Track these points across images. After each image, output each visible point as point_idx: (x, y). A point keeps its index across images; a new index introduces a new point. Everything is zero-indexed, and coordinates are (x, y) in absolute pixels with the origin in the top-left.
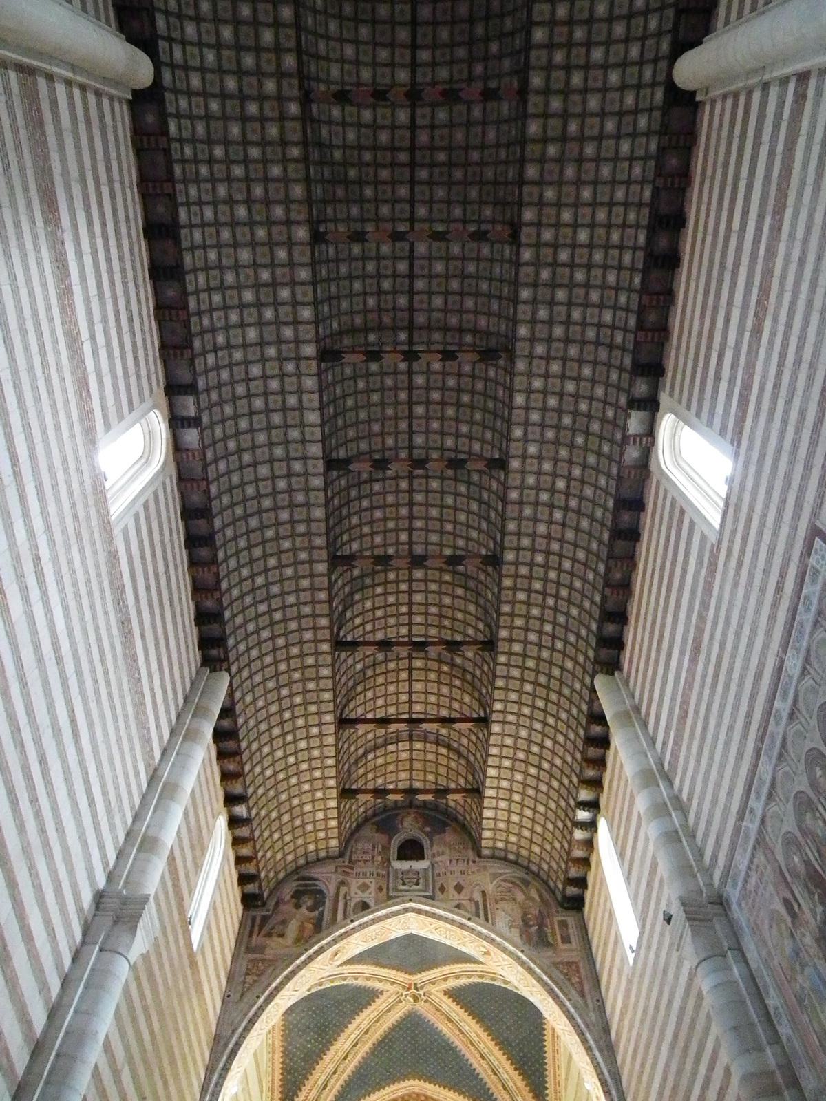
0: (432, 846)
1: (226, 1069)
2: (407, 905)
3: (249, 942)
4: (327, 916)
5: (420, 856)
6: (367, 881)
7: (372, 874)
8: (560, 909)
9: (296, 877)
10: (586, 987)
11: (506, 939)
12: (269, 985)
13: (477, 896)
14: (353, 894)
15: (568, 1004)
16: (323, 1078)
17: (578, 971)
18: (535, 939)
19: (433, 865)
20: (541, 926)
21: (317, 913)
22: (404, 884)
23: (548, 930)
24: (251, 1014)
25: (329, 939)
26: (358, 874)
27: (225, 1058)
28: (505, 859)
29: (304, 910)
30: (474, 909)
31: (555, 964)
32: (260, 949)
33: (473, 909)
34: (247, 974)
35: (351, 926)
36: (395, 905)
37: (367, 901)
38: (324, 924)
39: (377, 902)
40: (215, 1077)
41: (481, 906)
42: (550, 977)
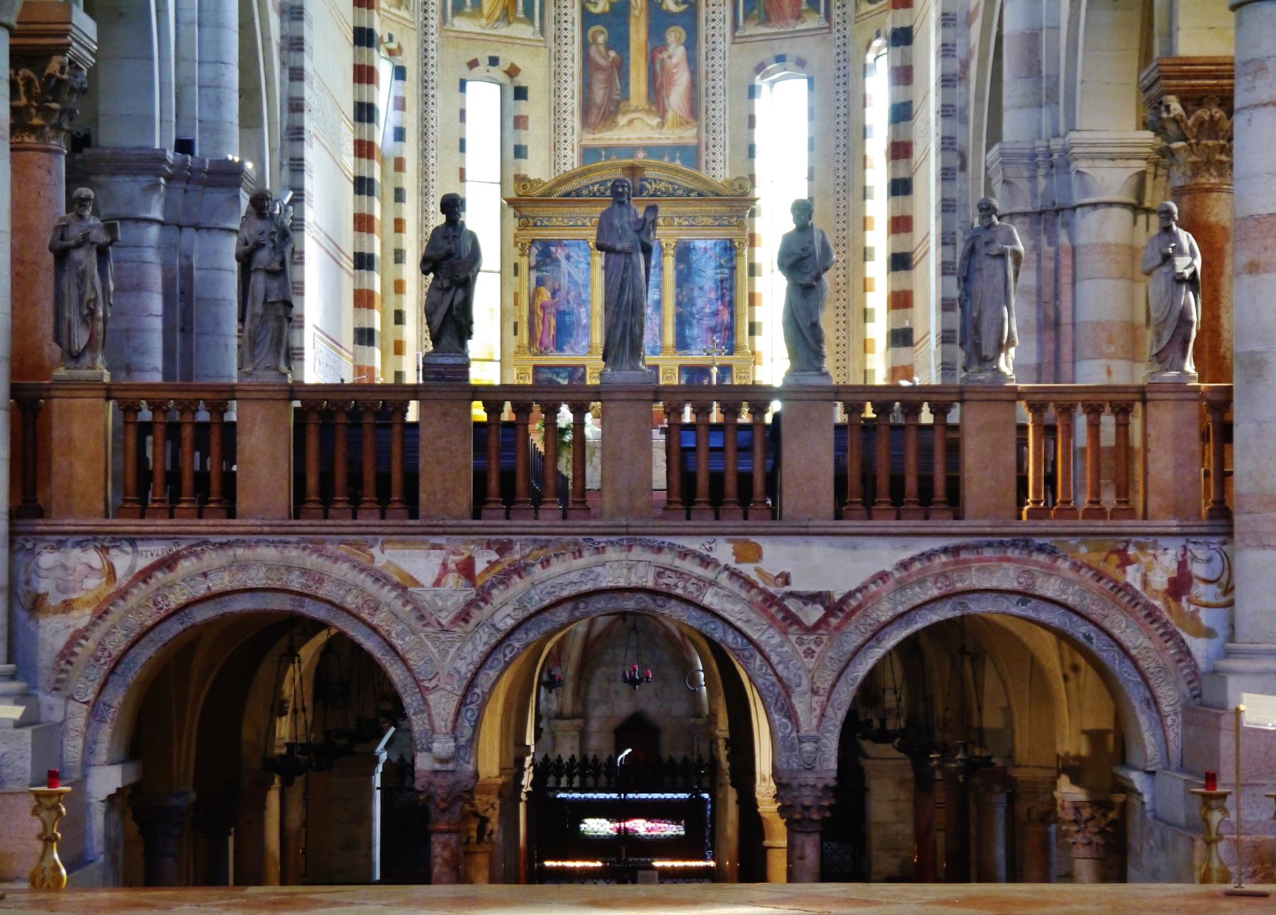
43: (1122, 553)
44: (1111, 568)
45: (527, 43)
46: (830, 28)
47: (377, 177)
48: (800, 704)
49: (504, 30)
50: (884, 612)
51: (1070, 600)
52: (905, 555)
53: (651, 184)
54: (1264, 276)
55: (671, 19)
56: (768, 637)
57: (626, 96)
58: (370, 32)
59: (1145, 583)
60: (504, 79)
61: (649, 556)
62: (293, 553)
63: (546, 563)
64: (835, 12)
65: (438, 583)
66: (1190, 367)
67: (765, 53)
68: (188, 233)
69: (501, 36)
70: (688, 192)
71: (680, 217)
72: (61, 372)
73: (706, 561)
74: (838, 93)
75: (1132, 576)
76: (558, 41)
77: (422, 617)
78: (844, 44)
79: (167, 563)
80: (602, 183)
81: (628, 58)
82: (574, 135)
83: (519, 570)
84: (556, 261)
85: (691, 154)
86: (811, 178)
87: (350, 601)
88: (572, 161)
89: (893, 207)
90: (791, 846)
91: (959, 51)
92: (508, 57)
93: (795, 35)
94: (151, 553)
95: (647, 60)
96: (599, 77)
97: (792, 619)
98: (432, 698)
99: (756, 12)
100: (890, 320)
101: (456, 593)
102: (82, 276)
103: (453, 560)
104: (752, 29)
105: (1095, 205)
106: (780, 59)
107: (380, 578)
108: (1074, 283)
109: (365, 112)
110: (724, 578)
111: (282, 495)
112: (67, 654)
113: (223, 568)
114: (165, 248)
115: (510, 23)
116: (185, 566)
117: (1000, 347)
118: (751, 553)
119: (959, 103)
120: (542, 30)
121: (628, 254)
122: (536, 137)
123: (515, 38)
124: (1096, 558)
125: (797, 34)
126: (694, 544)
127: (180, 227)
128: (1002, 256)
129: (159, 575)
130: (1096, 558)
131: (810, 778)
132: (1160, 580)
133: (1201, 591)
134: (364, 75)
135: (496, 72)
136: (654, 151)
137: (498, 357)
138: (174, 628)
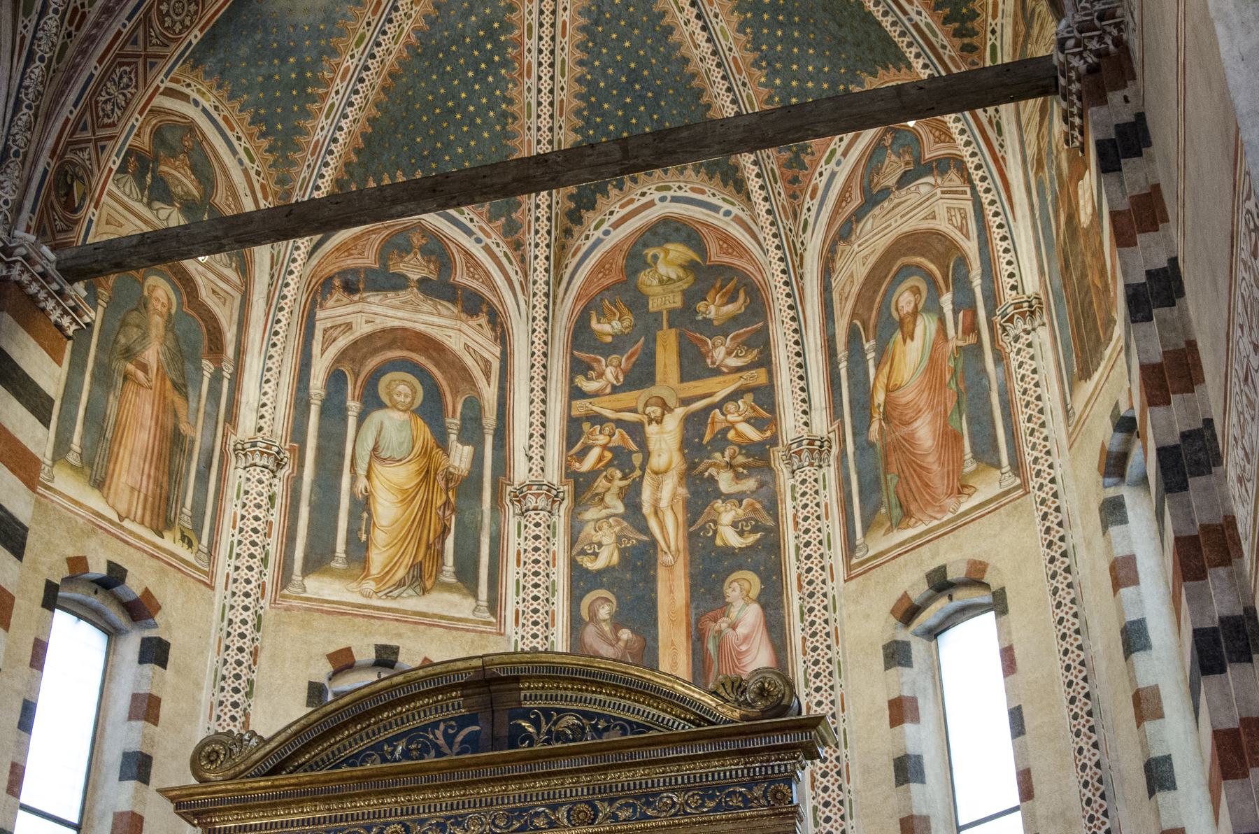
45: (460, 625)
46: (1024, 485)
49: (411, 602)
53: (536, 723)
55: (732, 560)
69: (405, 612)
71: (611, 801)
74: (1055, 591)
76: (521, 620)
78: (1055, 495)
81: (656, 639)
93: (959, 523)
95: (689, 636)
99: (883, 510)
104: (880, 542)
115: (425, 591)
120: (494, 605)
123: (434, 616)
125: (960, 522)
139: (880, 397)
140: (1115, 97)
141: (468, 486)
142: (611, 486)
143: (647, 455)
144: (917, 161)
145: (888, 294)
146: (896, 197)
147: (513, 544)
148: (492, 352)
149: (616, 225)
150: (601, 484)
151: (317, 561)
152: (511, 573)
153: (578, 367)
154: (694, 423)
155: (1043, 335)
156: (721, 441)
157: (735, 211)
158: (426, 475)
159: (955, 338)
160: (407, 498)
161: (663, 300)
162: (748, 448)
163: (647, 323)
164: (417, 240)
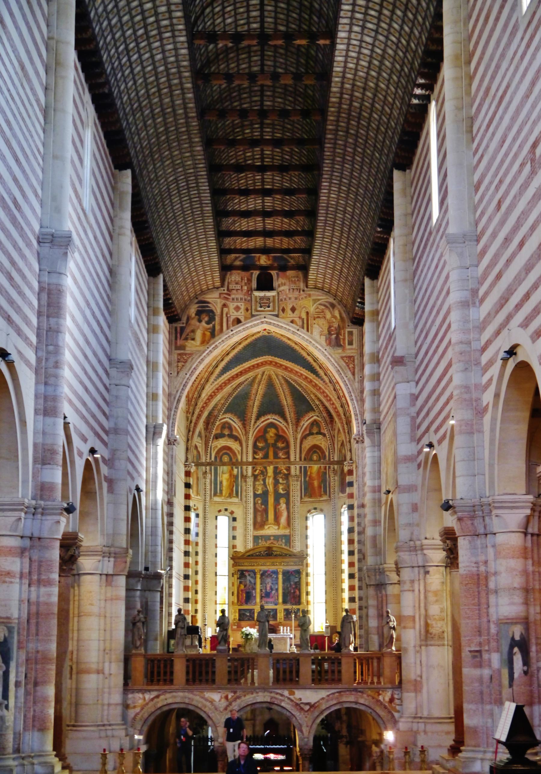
0: (278, 279)
1: (177, 408)
2: (263, 320)
3: (176, 343)
4: (217, 328)
5: (270, 288)
6: (239, 304)
7: (241, 299)
8: (350, 324)
9: (196, 301)
10: (356, 370)
11: (317, 342)
12: (191, 367)
13: (304, 316)
14: (231, 314)
15: (345, 379)
16: (215, 362)
17: (354, 361)
18: (333, 342)
19: (278, 293)
20: (338, 334)
21: (211, 325)
22: (261, 307)
23: (341, 337)
24: (184, 382)
25: (220, 341)
26: (233, 299)
27: (175, 403)
28: (322, 290)
29: (203, 323)
30: (301, 323)
31: (342, 358)
32: (183, 347)
33: (299, 322)
34: (178, 362)
35: (232, 333)
36: (256, 320)
37: (240, 317)
38: (216, 333)
39: (246, 318)
40: (173, 413)
41: (305, 322)
42: (338, 364)
43: (378, 692)
44: (376, 696)
47: (191, 550)
48: (305, 729)
49: (229, 500)
50: (324, 707)
51: (367, 703)
52: (328, 693)
54: (407, 630)
55: (282, 496)
56: (297, 713)
57: (267, 520)
58: (189, 506)
59: (384, 699)
60: (230, 515)
61: (269, 694)
62: (186, 694)
63: (245, 696)
64: (332, 495)
65: (220, 701)
66: (394, 648)
67: (310, 507)
68: (147, 592)
70: (286, 555)
72: (134, 652)
73: (282, 695)
75: (381, 698)
77: (216, 709)
79: (157, 697)
80: (260, 552)
82: (251, 532)
83: (239, 697)
84: (245, 576)
85: (288, 539)
86: (325, 546)
87: (200, 705)
88: (250, 545)
89: (349, 559)
90: (303, 764)
91: (363, 525)
92: (230, 508)
93: (320, 501)
94: (154, 694)
96: (259, 514)
97: (302, 709)
98: (218, 728)
100: (349, 594)
101: (224, 703)
102: (139, 629)
103: (224, 695)
104: (306, 499)
105: (391, 584)
106: (315, 509)
107: (206, 700)
108: (387, 604)
109: (187, 531)
110: (286, 699)
111: (184, 681)
112: (134, 719)
113: (170, 698)
114: (141, 596)
116: (162, 697)
117: (350, 644)
118: (293, 693)
119: (362, 540)
120: (241, 500)
121: (264, 622)
122: (239, 534)
124: (372, 694)
126: (279, 691)
127: (145, 591)
128: (350, 622)
129: (156, 700)
130: (372, 694)
131: (306, 747)
132: (387, 699)
133: (397, 702)
134: (187, 520)
135: (226, 513)
136: (277, 538)
137: (227, 602)
138: (159, 712)
139: (309, 473)
140: (351, 477)
141: (236, 477)
142: (261, 478)
143: (267, 473)
144: (320, 430)
145: (312, 454)
146: (316, 436)
147: (244, 488)
148: (239, 449)
149: (262, 422)
150: (259, 477)
151: (215, 494)
152: (244, 493)
153: (255, 453)
154: (276, 469)
155: (336, 478)
156: (280, 473)
157: (285, 424)
158: (230, 475)
159: (322, 470)
160: (228, 480)
161: (271, 441)
162: (285, 474)
163: (267, 446)
164: (227, 425)
